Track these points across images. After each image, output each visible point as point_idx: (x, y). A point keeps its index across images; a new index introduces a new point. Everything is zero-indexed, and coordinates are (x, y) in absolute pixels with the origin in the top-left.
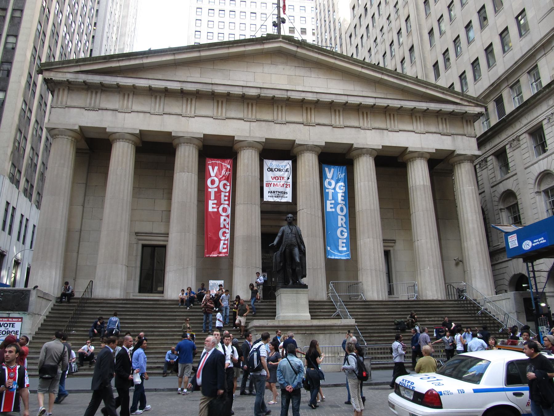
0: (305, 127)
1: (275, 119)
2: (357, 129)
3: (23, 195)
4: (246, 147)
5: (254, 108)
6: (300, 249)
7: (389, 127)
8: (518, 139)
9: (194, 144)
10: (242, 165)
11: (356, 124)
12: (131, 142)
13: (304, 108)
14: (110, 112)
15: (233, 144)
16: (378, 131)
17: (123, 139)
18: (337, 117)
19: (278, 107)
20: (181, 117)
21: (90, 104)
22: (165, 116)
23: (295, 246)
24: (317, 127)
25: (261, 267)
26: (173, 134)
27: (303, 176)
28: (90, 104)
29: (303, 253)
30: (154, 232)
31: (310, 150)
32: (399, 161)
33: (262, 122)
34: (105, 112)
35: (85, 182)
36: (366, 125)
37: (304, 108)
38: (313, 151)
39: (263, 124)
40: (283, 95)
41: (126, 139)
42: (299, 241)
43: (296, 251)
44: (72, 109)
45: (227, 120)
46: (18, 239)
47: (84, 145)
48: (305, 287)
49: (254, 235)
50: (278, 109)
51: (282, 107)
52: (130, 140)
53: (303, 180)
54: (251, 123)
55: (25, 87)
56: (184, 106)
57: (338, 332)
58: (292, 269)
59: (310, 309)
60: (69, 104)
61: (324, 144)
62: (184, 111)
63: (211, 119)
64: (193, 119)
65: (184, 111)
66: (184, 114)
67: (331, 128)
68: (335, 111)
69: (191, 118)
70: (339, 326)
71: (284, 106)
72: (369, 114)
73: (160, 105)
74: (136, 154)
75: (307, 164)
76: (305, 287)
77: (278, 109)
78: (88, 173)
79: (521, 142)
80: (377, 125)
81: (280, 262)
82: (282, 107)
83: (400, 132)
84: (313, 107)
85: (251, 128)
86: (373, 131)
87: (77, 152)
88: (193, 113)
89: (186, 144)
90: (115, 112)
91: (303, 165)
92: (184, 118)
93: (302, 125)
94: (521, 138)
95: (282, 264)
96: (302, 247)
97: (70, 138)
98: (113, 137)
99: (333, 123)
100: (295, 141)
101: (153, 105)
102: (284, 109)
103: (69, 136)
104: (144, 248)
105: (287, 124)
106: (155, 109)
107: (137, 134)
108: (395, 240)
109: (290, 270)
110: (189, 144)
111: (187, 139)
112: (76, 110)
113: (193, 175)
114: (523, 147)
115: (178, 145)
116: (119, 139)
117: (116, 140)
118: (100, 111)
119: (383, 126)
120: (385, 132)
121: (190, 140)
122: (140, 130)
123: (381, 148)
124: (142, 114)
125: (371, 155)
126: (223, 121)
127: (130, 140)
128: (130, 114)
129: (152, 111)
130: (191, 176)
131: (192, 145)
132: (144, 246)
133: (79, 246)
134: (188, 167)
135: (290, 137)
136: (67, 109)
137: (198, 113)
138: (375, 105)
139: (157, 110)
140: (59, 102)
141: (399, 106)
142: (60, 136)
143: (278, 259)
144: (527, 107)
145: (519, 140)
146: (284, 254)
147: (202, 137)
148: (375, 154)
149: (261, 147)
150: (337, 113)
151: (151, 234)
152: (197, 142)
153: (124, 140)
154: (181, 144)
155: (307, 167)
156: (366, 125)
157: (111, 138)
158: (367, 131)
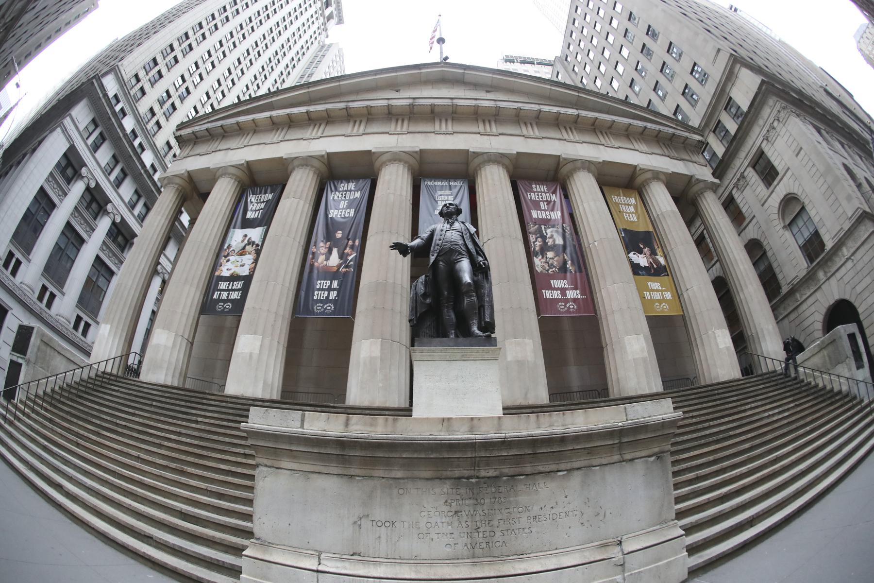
8: (742, 176)
9: (312, 166)
11: (559, 136)
19: (441, 120)
40: (449, 102)
43: (465, 265)
49: (392, 280)
51: (446, 120)
79: (748, 179)
81: (425, 295)
82: (446, 120)
94: (746, 174)
95: (428, 301)
109: (453, 316)
113: (302, 202)
114: (751, 183)
125: (589, 171)
130: (298, 202)
134: (295, 192)
144: (735, 143)
145: (744, 177)
150: (529, 126)
152: (317, 163)
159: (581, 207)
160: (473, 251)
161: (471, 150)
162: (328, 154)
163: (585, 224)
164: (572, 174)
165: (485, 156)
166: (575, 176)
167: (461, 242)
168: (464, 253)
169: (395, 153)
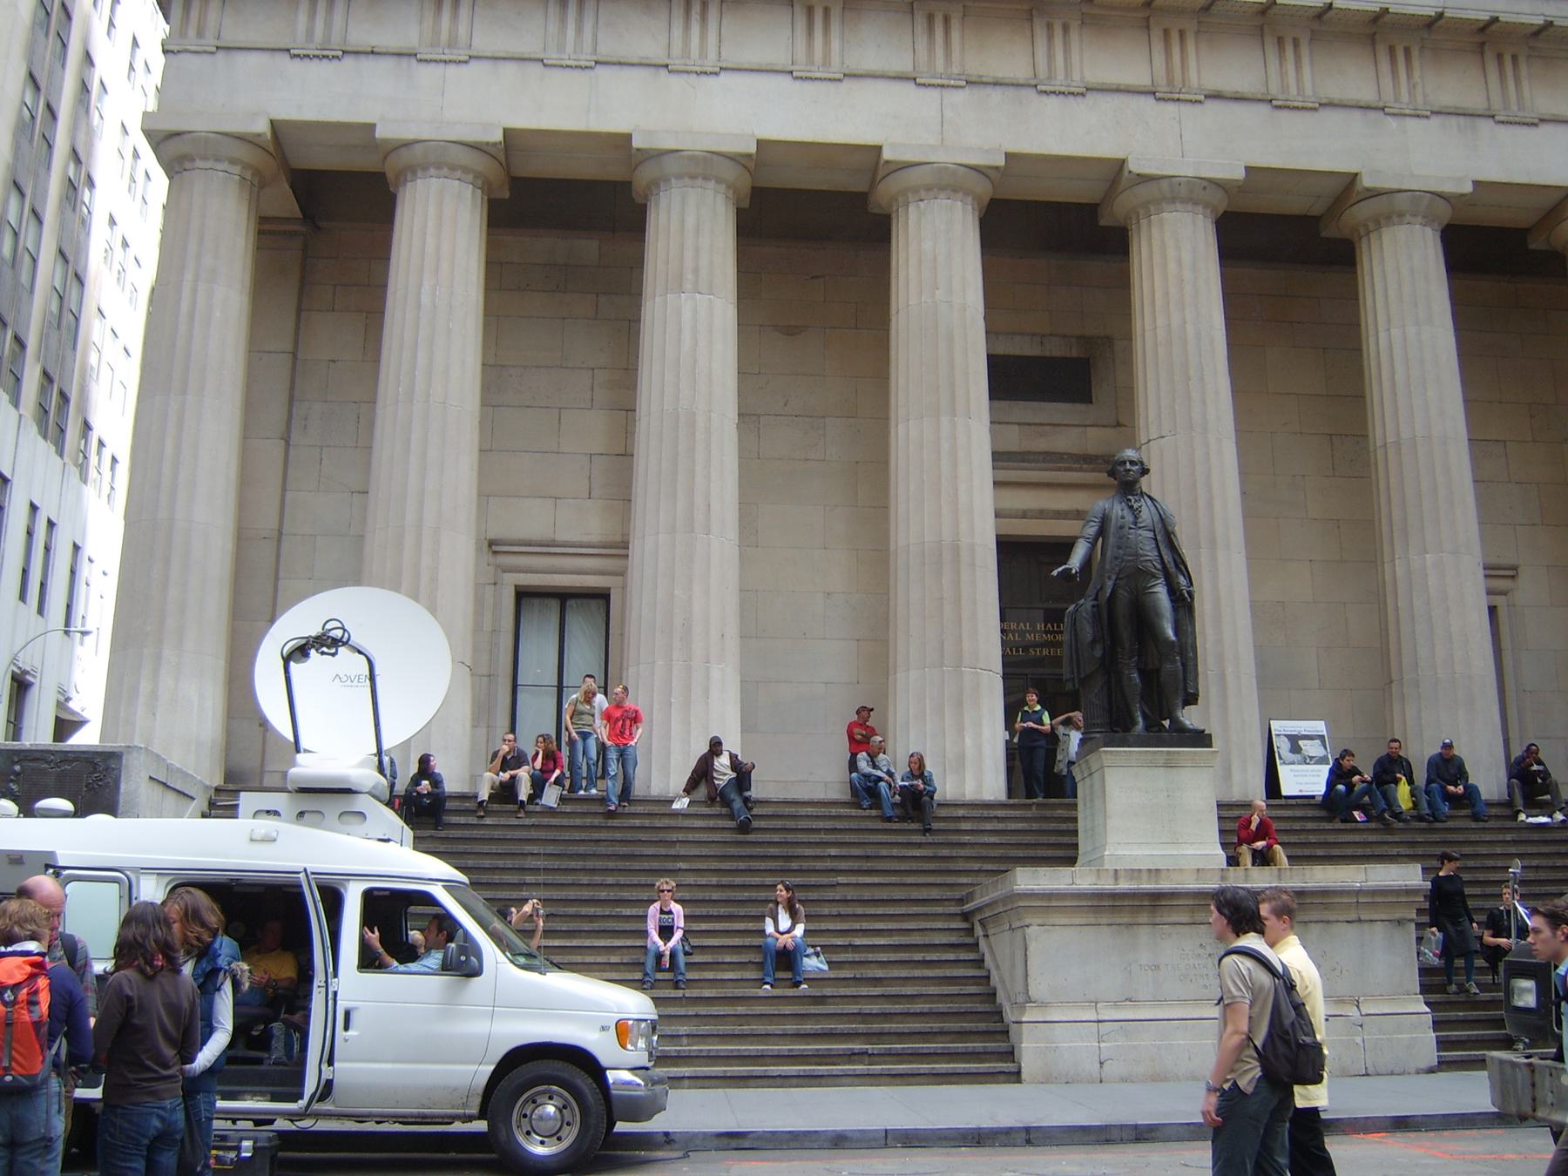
0: (1162, 105)
1: (1042, 71)
2: (1372, 115)
3: (35, 428)
4: (929, 189)
5: (955, 35)
6: (1173, 591)
7: (1497, 103)
9: (719, 181)
10: (913, 261)
11: (1367, 94)
12: (470, 177)
13: (1156, 34)
14: (387, 64)
15: (873, 183)
16: (1454, 120)
17: (439, 167)
18: (1290, 66)
19: (1050, 27)
20: (663, 72)
21: (310, 33)
22: (600, 70)
23: (1154, 576)
24: (1211, 106)
25: (999, 667)
26: (636, 143)
27: (1159, 302)
28: (310, 33)
29: (1183, 603)
30: (561, 537)
31: (1184, 201)
32: (1532, 246)
33: (989, 90)
34: (368, 64)
35: (289, 347)
36: (1405, 96)
37: (1156, 34)
38: (1196, 203)
39: (996, 95)
41: (453, 168)
42: (1167, 557)
44: (240, 58)
45: (848, 84)
46: (23, 596)
47: (283, 202)
48: (1201, 739)
50: (1050, 37)
51: (1066, 29)
52: (466, 170)
53: (1159, 322)
54: (946, 92)
55: (35, 23)
56: (677, 31)
57: (1353, 916)
58: (1141, 672)
59: (1221, 832)
60: (229, 38)
61: (1239, 174)
62: (677, 49)
63: (785, 81)
64: (712, 79)
65: (677, 49)
66: (676, 63)
67: (1264, 109)
68: (1280, 41)
69: (704, 78)
70: (1359, 892)
71: (1075, 25)
72: (1415, 53)
73: (579, 30)
74: (488, 234)
75: (1171, 253)
76: (1201, 739)
77: (1050, 37)
78: (299, 311)
80: (1446, 99)
81: (1094, 641)
82: (1066, 29)
83: (1545, 129)
84: (1190, 26)
85: (948, 114)
86: (1435, 120)
87: (260, 233)
88: (712, 55)
89: (687, 181)
90: (405, 60)
91: (1157, 259)
92: (676, 81)
93: (1150, 100)
95: (1098, 653)
96: (1182, 580)
97: (236, 169)
98: (405, 156)
99: (1274, 90)
100: (1123, 162)
101: (553, 28)
102: (1074, 35)
103: (233, 161)
104: (524, 601)
105: (1091, 97)
106: (561, 48)
107: (495, 144)
108: (1515, 568)
110: (699, 182)
111: (693, 159)
112: (253, 59)
115: (655, 184)
116: (425, 168)
117: (411, 171)
118: (349, 62)
119: (1475, 101)
120: (1485, 126)
121: (702, 166)
122: (506, 131)
123: (1468, 188)
124: (510, 69)
125: (1428, 220)
126: (832, 86)
127: (466, 170)
128: (463, 68)
129: (552, 56)
131: (712, 184)
132: (524, 596)
133: (275, 597)
134: (696, 271)
135: (1103, 146)
136: (221, 55)
137: (732, 56)
138: (1440, 16)
139: (570, 47)
140: (192, 32)
141: (1539, 21)
142: (199, 164)
143: (1087, 632)
146: (1106, 615)
147: (753, 149)
148: (1445, 213)
149: (985, 190)
151: (547, 546)
153: (445, 171)
154: (667, 180)
155: (1172, 267)
156: (1405, 96)
157: (390, 170)
158: (1412, 123)
159: (1382, 335)
160: (1172, 569)
161: (1134, 166)
162: (761, 143)
163: (1386, 385)
164: (1379, 226)
165: (1165, 184)
166: (1387, 234)
167: (1153, 555)
168: (1160, 574)
169: (942, 170)
